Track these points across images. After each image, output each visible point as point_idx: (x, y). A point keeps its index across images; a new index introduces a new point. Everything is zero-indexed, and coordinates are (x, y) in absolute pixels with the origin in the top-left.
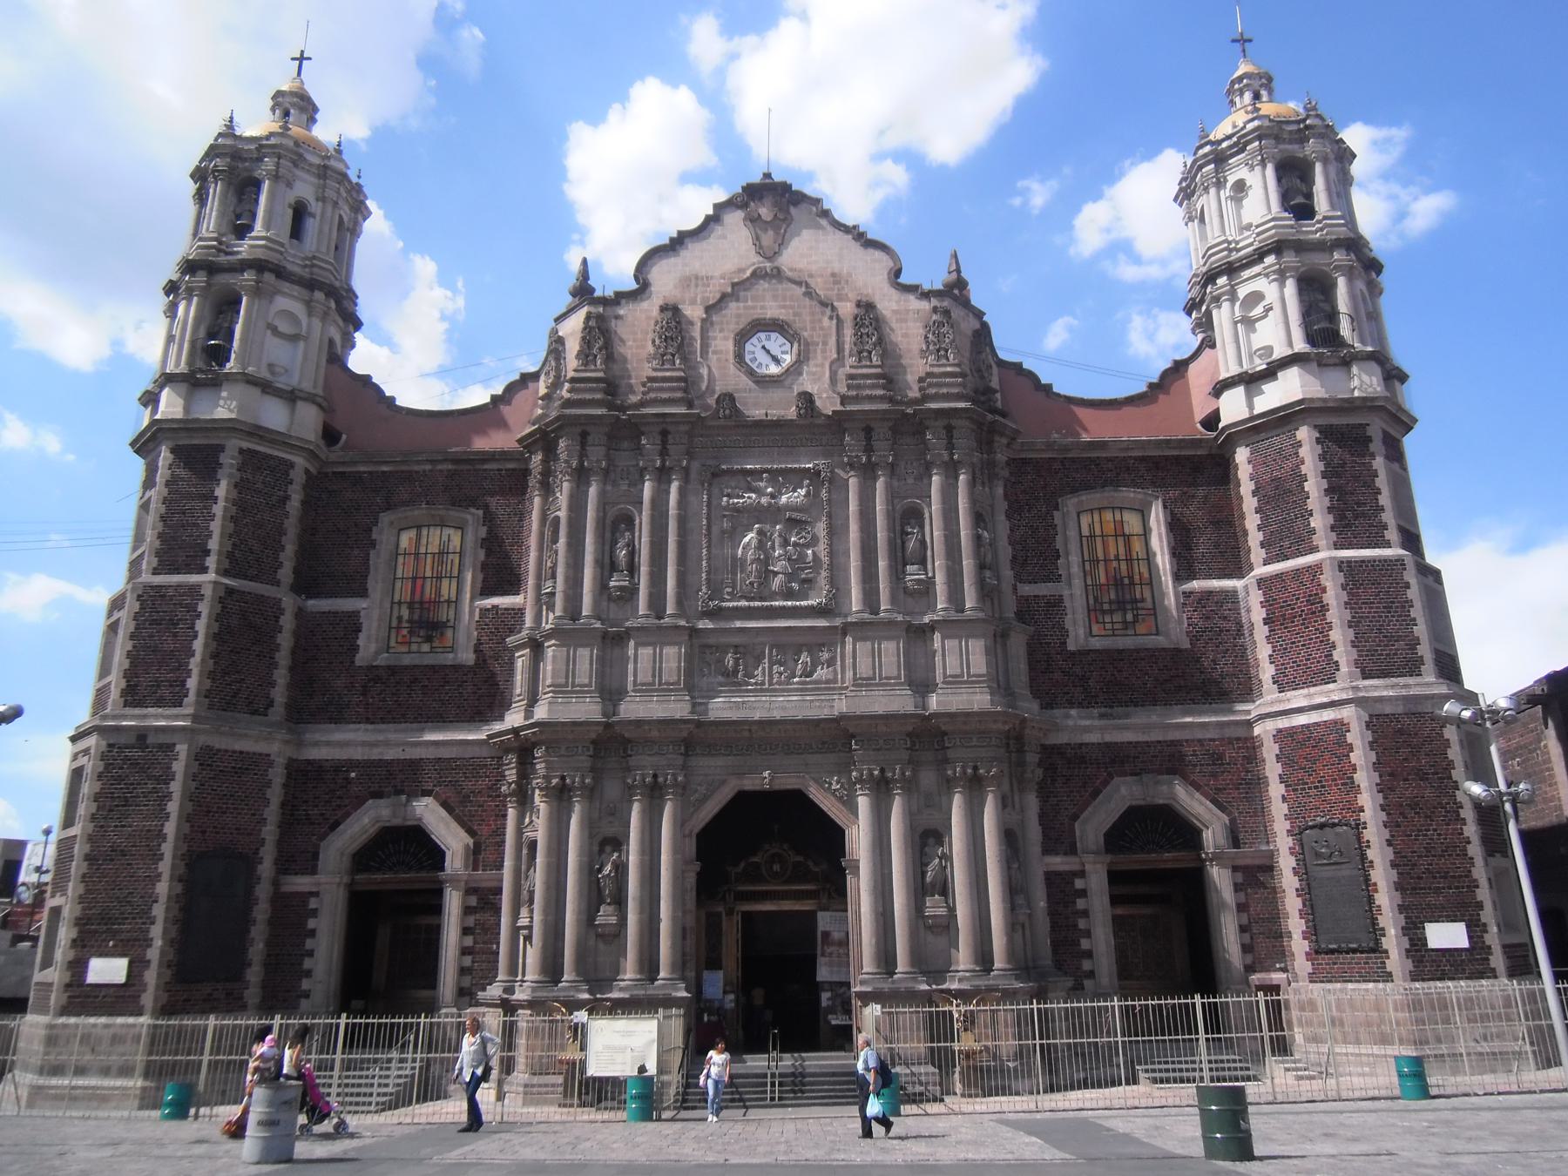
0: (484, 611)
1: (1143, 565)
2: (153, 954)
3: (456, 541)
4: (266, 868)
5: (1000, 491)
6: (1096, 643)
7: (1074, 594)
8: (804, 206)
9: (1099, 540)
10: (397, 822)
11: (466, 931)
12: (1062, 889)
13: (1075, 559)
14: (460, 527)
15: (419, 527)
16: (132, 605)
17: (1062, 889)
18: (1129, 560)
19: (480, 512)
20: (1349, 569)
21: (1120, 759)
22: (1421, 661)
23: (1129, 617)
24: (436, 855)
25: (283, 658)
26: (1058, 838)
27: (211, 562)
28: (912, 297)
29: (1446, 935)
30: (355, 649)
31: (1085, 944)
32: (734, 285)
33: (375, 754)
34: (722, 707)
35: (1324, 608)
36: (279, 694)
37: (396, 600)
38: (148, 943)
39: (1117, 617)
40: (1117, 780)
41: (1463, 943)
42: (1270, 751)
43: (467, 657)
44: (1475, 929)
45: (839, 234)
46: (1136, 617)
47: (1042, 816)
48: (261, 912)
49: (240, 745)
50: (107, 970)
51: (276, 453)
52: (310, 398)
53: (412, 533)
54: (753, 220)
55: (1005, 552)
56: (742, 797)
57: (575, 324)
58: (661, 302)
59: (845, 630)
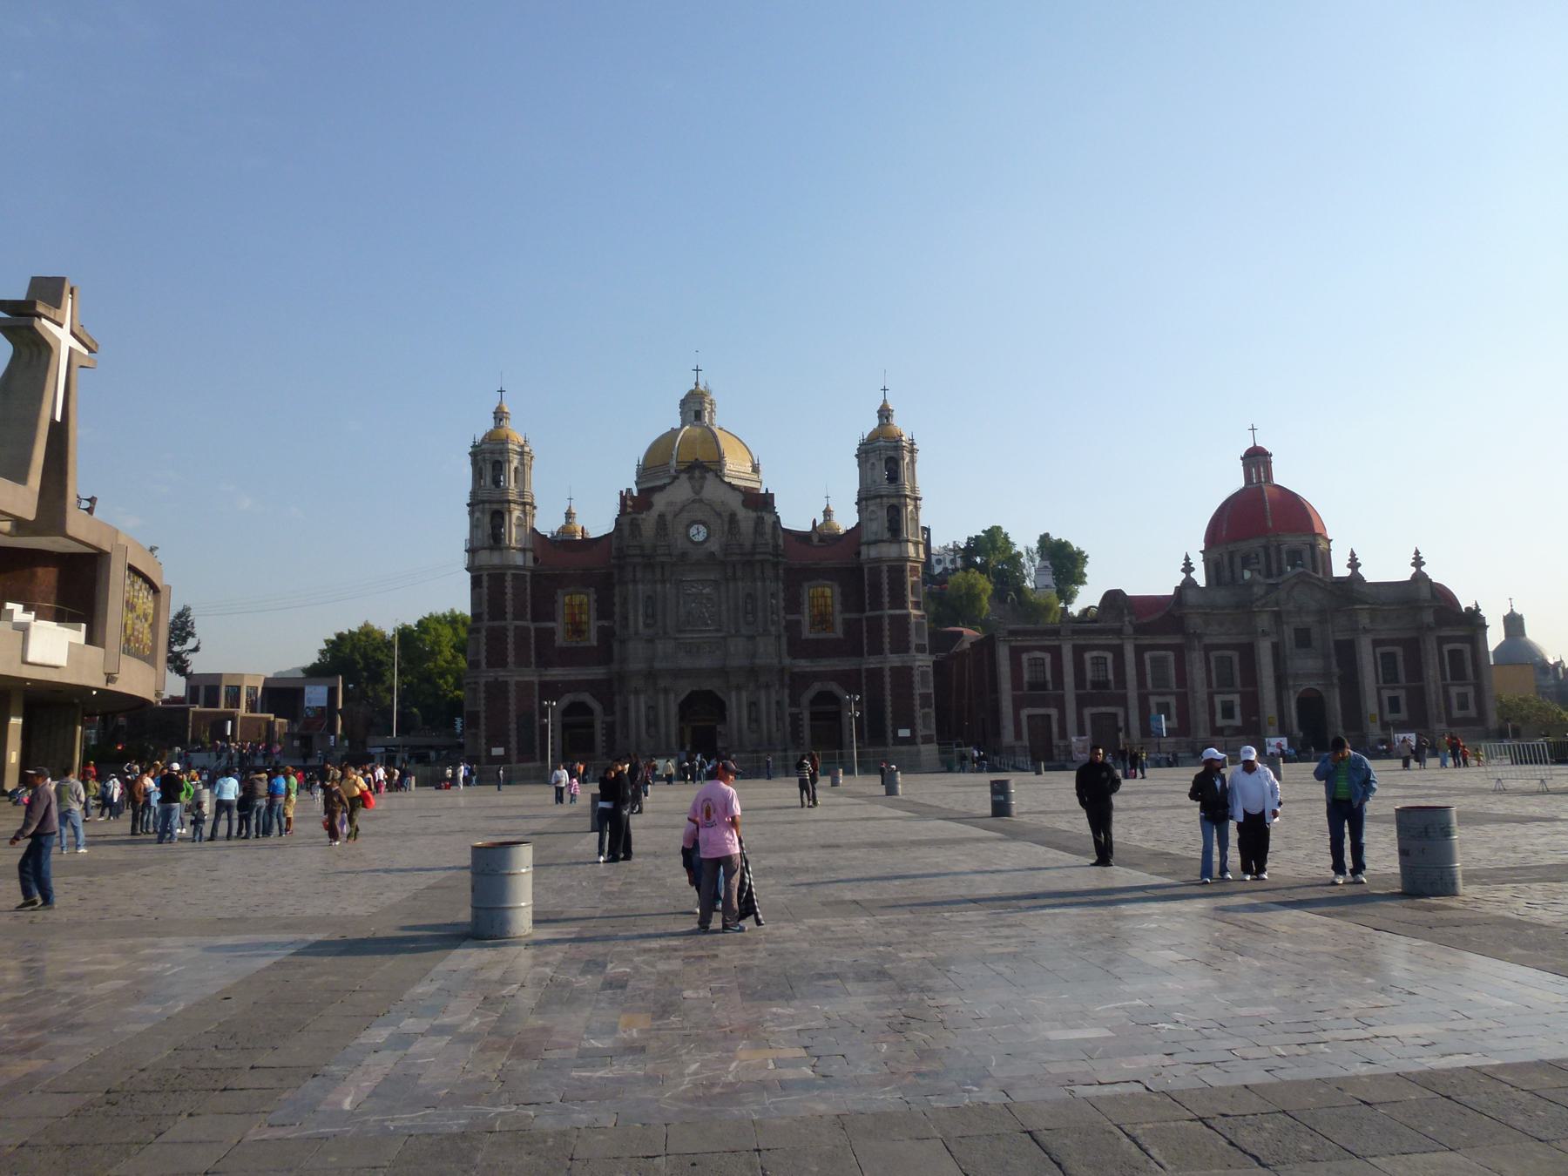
0: (599, 627)
1: (830, 608)
2: (511, 746)
3: (586, 600)
4: (537, 718)
5: (781, 585)
6: (812, 636)
7: (806, 620)
8: (711, 473)
9: (815, 599)
10: (577, 700)
11: (603, 735)
12: (795, 719)
13: (806, 606)
14: (588, 595)
15: (571, 595)
16: (484, 633)
17: (795, 719)
18: (825, 606)
19: (593, 589)
20: (892, 617)
21: (816, 676)
22: (909, 648)
23: (824, 627)
24: (590, 711)
25: (533, 647)
26: (794, 702)
27: (509, 616)
28: (750, 511)
29: (904, 733)
30: (554, 641)
31: (801, 735)
32: (684, 506)
33: (567, 678)
34: (686, 662)
35: (882, 630)
36: (533, 660)
37: (566, 621)
38: (509, 743)
39: (820, 627)
40: (815, 683)
41: (908, 735)
42: (864, 675)
43: (595, 643)
44: (913, 732)
45: (726, 486)
46: (827, 627)
47: (790, 696)
48: (537, 732)
49: (526, 679)
50: (498, 751)
51: (522, 572)
52: (531, 550)
53: (569, 597)
54: (691, 478)
55: (782, 604)
56: (693, 693)
57: (626, 519)
58: (657, 513)
59: (724, 638)
